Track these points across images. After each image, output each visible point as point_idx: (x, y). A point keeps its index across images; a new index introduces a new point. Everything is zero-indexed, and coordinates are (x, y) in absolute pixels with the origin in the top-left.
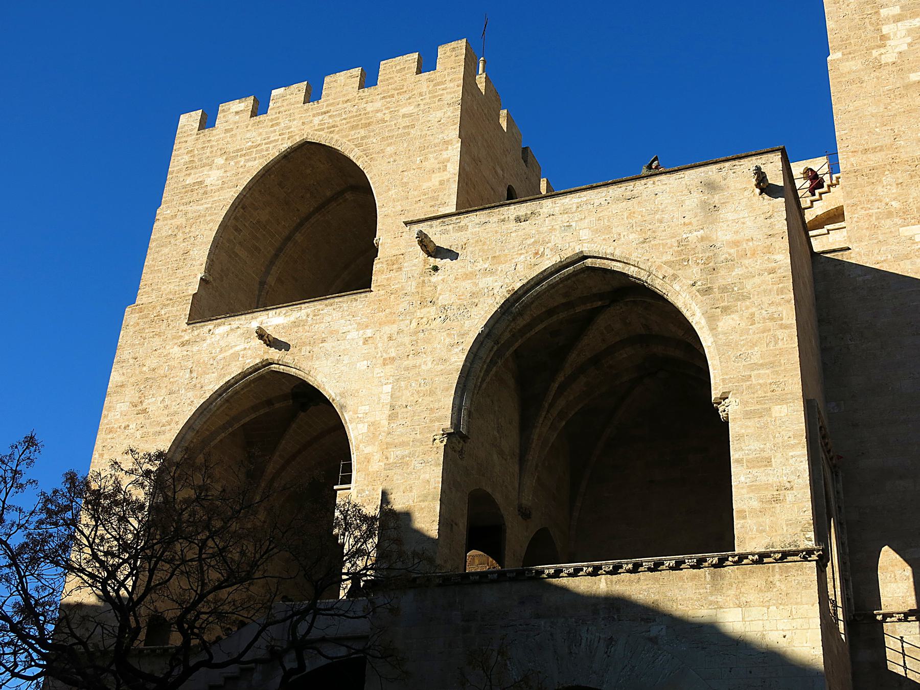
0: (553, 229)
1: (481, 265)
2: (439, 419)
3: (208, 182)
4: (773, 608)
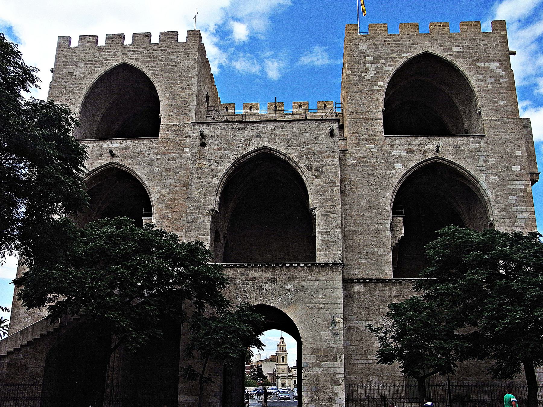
0: (253, 136)
1: (224, 145)
3: (75, 73)
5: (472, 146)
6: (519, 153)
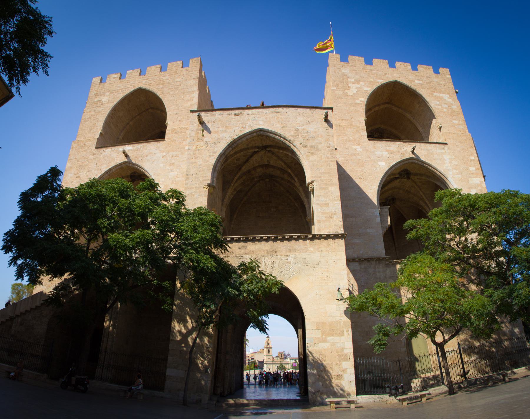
2: (206, 180)
4: (330, 253)
5: (438, 151)
6: (473, 158)
